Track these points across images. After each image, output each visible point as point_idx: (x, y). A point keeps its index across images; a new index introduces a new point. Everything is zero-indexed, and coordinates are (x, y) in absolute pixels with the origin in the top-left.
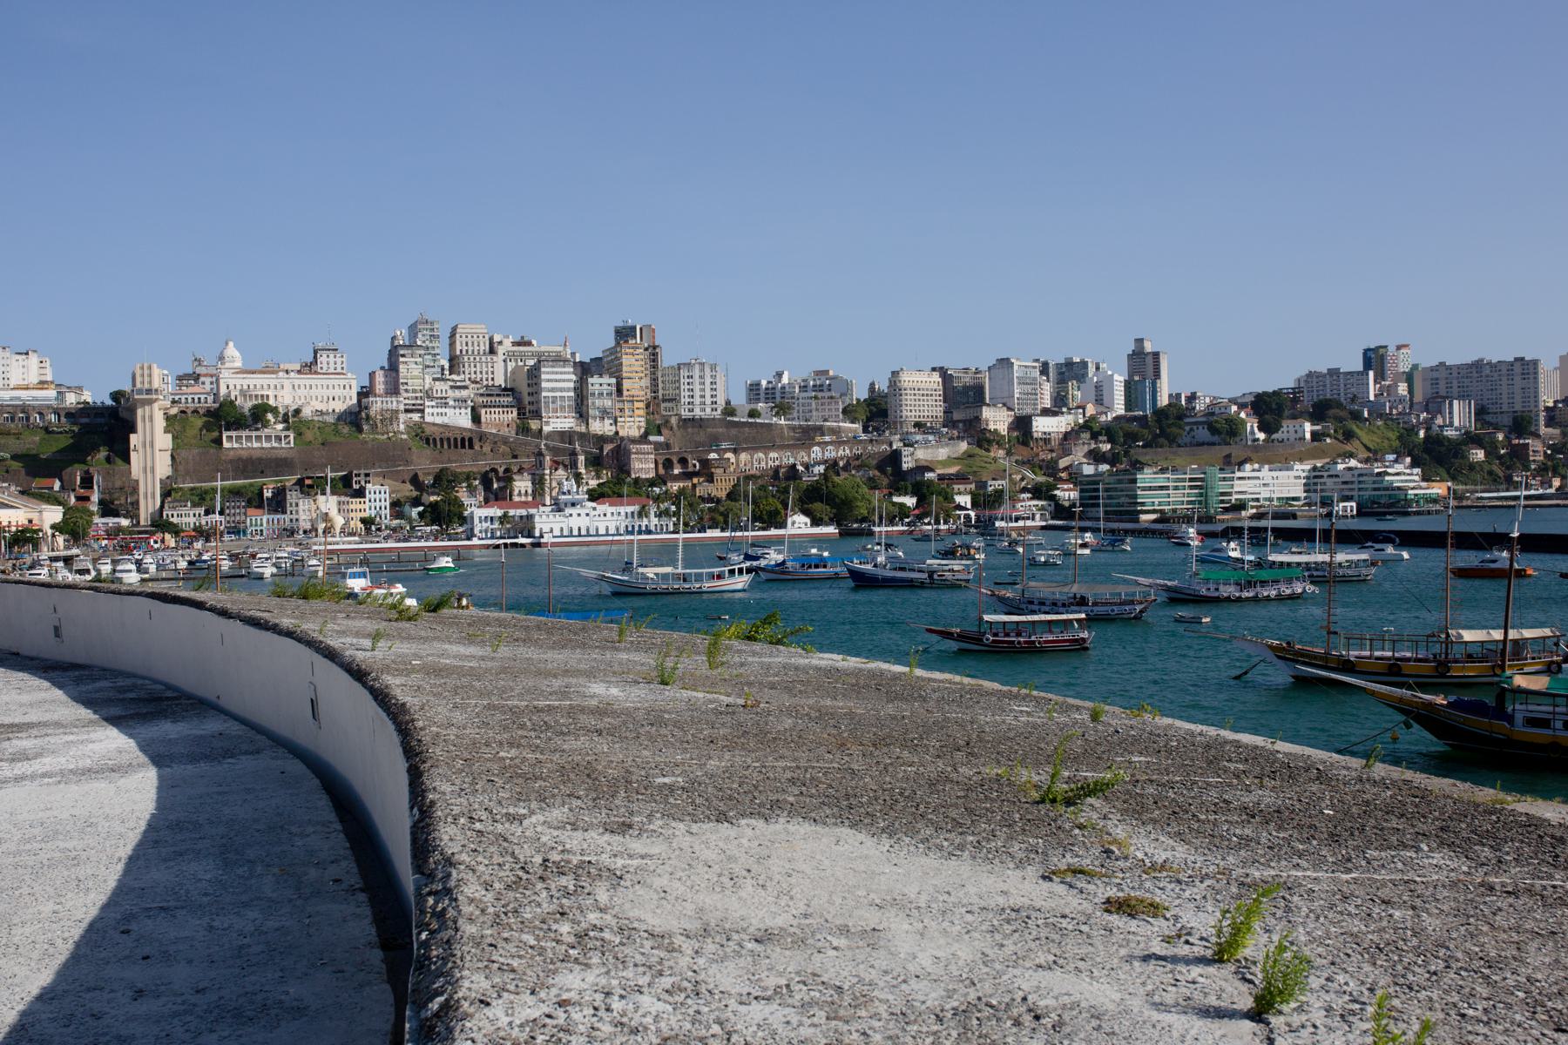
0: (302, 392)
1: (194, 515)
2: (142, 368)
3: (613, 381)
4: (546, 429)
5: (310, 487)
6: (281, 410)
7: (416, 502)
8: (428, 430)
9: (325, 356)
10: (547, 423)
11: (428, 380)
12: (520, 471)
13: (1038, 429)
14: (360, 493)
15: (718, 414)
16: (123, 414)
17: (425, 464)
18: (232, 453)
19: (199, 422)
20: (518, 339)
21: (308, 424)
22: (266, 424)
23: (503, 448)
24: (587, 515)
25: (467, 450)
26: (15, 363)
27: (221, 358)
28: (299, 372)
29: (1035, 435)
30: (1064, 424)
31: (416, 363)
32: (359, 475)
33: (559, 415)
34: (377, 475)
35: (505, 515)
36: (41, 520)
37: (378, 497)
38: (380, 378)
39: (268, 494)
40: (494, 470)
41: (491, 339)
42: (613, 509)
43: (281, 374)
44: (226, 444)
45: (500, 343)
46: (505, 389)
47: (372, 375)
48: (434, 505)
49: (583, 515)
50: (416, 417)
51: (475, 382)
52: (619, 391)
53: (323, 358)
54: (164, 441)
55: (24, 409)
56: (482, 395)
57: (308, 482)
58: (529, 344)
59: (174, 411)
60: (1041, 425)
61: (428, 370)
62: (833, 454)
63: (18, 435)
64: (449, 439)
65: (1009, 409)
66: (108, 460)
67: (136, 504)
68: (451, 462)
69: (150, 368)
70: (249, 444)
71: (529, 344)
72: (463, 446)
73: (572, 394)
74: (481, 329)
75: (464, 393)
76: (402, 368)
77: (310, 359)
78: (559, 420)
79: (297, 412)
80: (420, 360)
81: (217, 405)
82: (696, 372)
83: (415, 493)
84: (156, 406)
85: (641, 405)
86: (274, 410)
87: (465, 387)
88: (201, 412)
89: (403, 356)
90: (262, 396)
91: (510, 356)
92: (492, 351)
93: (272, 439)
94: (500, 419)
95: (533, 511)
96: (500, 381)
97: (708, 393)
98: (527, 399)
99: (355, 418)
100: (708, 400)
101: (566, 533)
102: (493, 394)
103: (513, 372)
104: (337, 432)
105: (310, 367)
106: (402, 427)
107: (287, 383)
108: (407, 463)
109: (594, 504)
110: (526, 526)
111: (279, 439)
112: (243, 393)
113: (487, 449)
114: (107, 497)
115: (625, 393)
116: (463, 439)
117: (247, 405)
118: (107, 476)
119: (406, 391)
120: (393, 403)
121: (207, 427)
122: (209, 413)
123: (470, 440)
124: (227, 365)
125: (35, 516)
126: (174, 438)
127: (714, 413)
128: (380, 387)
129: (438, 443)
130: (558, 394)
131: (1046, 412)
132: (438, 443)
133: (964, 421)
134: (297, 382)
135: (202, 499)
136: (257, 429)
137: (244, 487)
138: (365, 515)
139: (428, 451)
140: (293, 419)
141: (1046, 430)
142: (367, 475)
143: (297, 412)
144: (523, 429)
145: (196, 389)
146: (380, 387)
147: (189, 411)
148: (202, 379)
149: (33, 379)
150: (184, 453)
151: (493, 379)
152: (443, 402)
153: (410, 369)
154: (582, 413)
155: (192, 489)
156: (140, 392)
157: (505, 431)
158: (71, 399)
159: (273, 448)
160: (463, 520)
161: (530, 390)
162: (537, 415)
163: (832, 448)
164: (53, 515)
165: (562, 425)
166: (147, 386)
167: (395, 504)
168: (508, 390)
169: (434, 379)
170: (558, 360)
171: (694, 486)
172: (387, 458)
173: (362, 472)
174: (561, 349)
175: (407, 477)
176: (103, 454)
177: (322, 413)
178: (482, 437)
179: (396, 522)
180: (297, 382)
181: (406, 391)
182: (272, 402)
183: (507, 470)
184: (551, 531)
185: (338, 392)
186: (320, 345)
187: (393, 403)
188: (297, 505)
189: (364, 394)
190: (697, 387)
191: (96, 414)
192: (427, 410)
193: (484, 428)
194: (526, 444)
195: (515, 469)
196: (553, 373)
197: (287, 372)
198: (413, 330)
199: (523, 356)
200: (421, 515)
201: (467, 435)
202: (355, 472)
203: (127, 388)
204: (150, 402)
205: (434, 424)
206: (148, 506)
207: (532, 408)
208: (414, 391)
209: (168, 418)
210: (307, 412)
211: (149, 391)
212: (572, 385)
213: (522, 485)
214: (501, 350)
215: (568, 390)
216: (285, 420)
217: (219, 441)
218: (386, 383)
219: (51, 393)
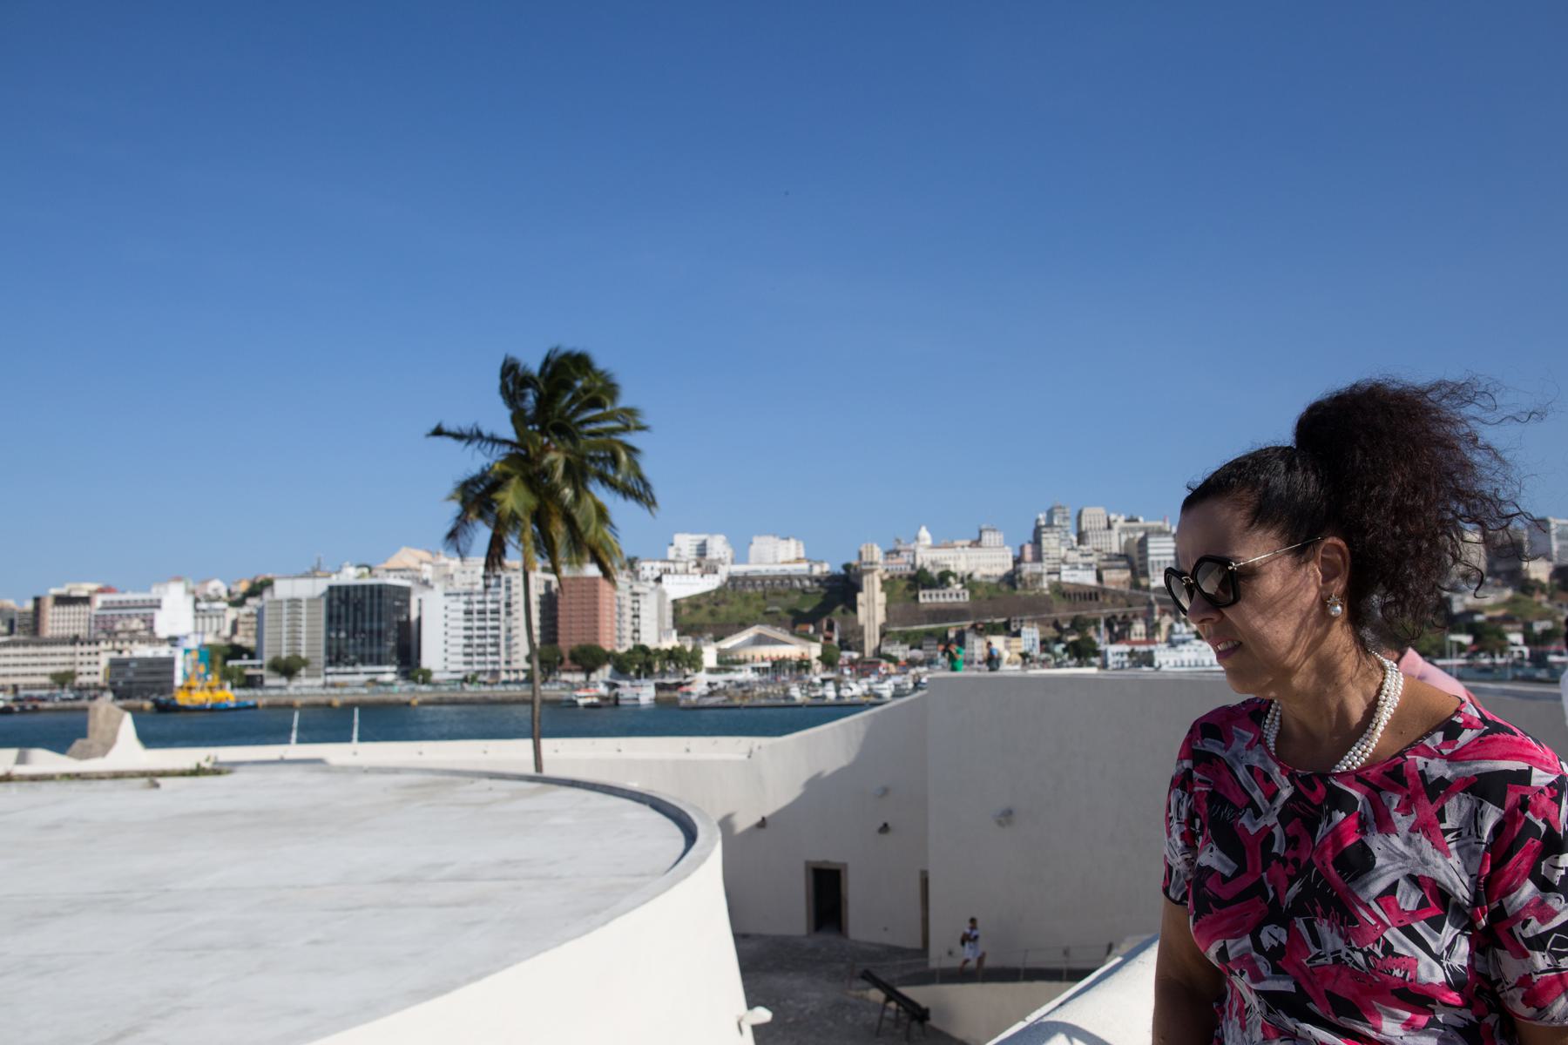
0: (973, 561)
2: (867, 547)
5: (981, 630)
6: (959, 575)
7: (1058, 641)
8: (1065, 588)
10: (1154, 581)
11: (1063, 550)
12: (1135, 617)
14: (1017, 634)
16: (853, 580)
17: (1063, 613)
19: (903, 585)
20: (1128, 517)
21: (978, 584)
22: (949, 585)
23: (1120, 600)
25: (1093, 602)
27: (917, 539)
28: (970, 546)
31: (1055, 538)
32: (1015, 621)
34: (1029, 621)
35: (1132, 651)
36: (809, 652)
37: (1031, 636)
38: (1028, 550)
39: (952, 635)
40: (1114, 617)
41: (1108, 519)
43: (959, 549)
44: (921, 600)
45: (1115, 521)
46: (1120, 556)
47: (1022, 548)
48: (1074, 644)
50: (1055, 578)
51: (1097, 550)
53: (986, 537)
54: (881, 598)
55: (789, 577)
56: (1104, 560)
57: (980, 626)
58: (1136, 520)
59: (886, 577)
61: (1063, 543)
63: (785, 595)
64: (1080, 594)
66: (844, 611)
67: (862, 643)
68: (1081, 610)
69: (872, 547)
71: (1136, 520)
72: (1091, 599)
74: (1101, 511)
75: (1090, 559)
76: (1044, 542)
77: (976, 537)
79: (970, 576)
80: (1057, 535)
81: (914, 572)
83: (1056, 634)
84: (876, 574)
86: (955, 575)
87: (1091, 555)
88: (905, 577)
89: (1045, 533)
90: (946, 565)
91: (1124, 530)
92: (1109, 527)
93: (955, 595)
94: (1117, 578)
95: (1152, 647)
96: (1116, 549)
98: (1137, 563)
99: (1011, 579)
101: (1179, 664)
102: (1113, 559)
103: (1126, 543)
104: (998, 590)
105: (977, 543)
106: (1045, 585)
107: (963, 555)
108: (1050, 611)
110: (1148, 659)
111: (958, 596)
112: (933, 563)
113: (1108, 600)
114: (843, 638)
116: (1090, 594)
117: (935, 572)
118: (843, 622)
119: (1048, 559)
120: (1038, 568)
121: (910, 588)
122: (910, 578)
123: (1096, 594)
124: (922, 543)
125: (805, 650)
126: (888, 596)
128: (1028, 554)
129: (1072, 597)
130: (1162, 558)
132: (1072, 597)
134: (969, 554)
135: (905, 638)
136: (943, 588)
137: (934, 630)
138: (1022, 650)
139: (1065, 603)
140: (968, 581)
142: (1021, 621)
143: (970, 576)
144: (1135, 585)
145: (899, 560)
146: (1028, 554)
147: (896, 577)
148: (902, 553)
149: (792, 556)
150: (893, 607)
151: (1110, 548)
152: (1074, 567)
153: (1050, 542)
155: (900, 632)
156: (866, 564)
157: (1122, 588)
158: (817, 570)
159: (954, 603)
160: (1097, 653)
162: (1145, 574)
164: (815, 650)
166: (870, 560)
167: (1044, 643)
168: (1120, 557)
169: (1068, 549)
170: (1161, 532)
172: (1036, 608)
173: (1018, 618)
174: (1160, 523)
175: (1051, 622)
176: (839, 608)
177: (987, 576)
178: (1105, 592)
179: (1044, 656)
180: (969, 554)
181: (1048, 559)
182: (952, 569)
183: (1124, 617)
184: (1167, 662)
185: (998, 560)
186: (984, 527)
187: (1038, 568)
188: (973, 643)
189: (1018, 561)
192: (1063, 573)
193: (1106, 586)
194: (1138, 596)
195: (1130, 615)
197: (963, 547)
198: (1050, 514)
199: (1133, 530)
200: (1065, 650)
201: (1093, 590)
202: (1013, 619)
203: (855, 561)
204: (872, 571)
205: (1068, 583)
206: (871, 642)
207: (1143, 569)
208: (1054, 559)
209: (883, 582)
210: (977, 576)
211: (871, 563)
212: (1172, 551)
213: (1139, 628)
214: (1116, 527)
216: (962, 581)
217: (916, 597)
218: (1033, 553)
219: (804, 567)
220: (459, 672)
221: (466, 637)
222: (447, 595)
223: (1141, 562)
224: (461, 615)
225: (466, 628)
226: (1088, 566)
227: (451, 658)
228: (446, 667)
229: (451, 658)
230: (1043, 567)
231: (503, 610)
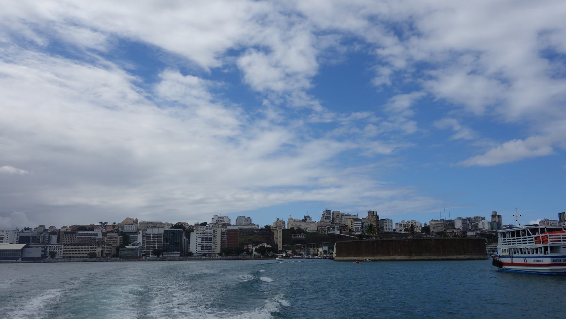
10: (356, 233)
30: (475, 233)
97: (390, 226)
100: (390, 228)
131: (470, 230)
141: (470, 235)
152: (334, 228)
190: (388, 225)
215: (360, 225)
220: (200, 254)
221: (202, 245)
222: (197, 233)
224: (201, 239)
225: (202, 242)
226: (337, 228)
227: (198, 250)
228: (196, 253)
229: (198, 250)
230: (326, 228)
231: (212, 238)
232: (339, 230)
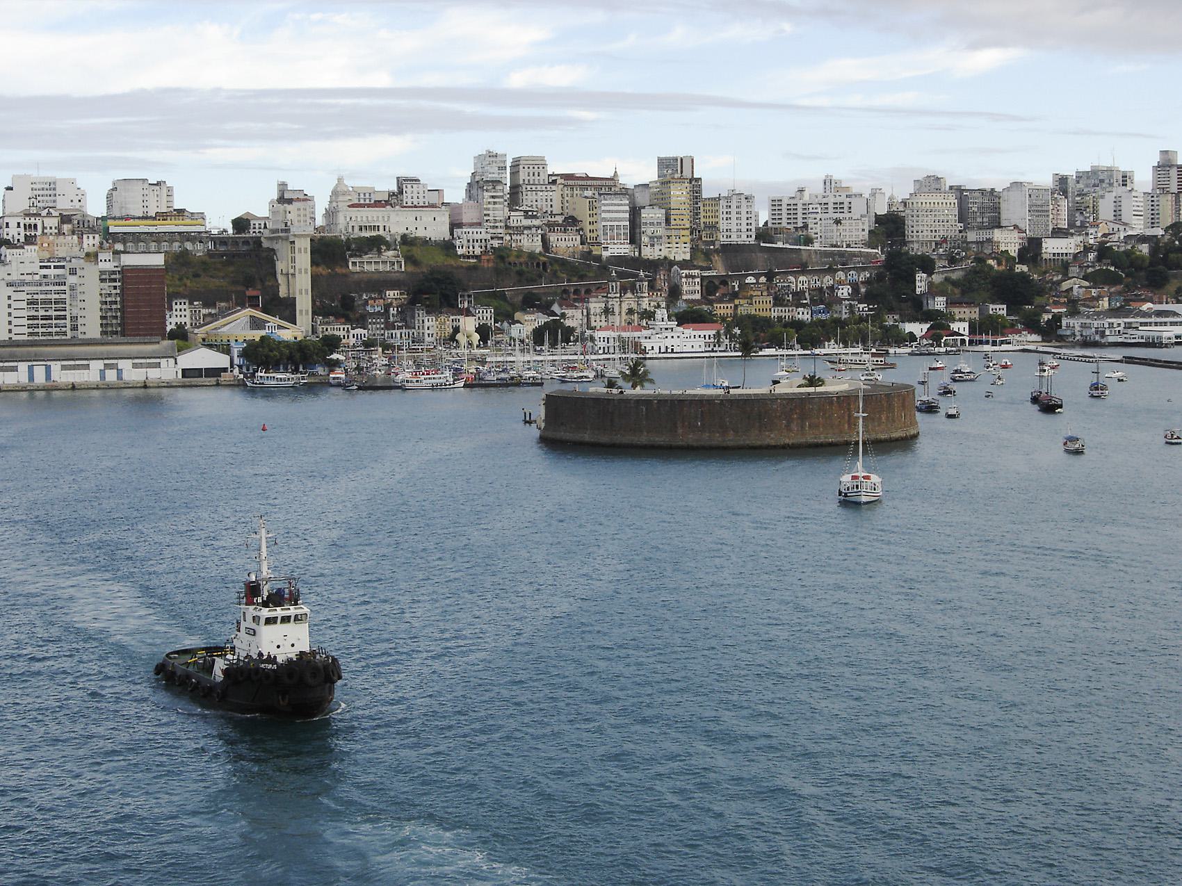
1: (344, 330)
3: (663, 211)
4: (605, 254)
9: (409, 186)
13: (1048, 250)
15: (752, 241)
18: (356, 276)
24: (678, 337)
26: (152, 193)
29: (1044, 256)
30: (1073, 246)
33: (616, 242)
42: (697, 333)
49: (675, 337)
52: (668, 221)
53: (408, 189)
60: (1052, 247)
62: (855, 277)
65: (1021, 231)
70: (355, 268)
73: (628, 223)
78: (616, 246)
82: (734, 204)
85: (688, 232)
93: (387, 262)
100: (744, 228)
109: (681, 329)
115: (673, 222)
127: (749, 239)
131: (1058, 233)
133: (977, 243)
141: (1056, 251)
154: (634, 239)
161: (591, 219)
163: (854, 272)
165: (619, 251)
171: (736, 306)
191: (243, 242)
196: (612, 205)
223: (591, 227)
232: (540, 236)
